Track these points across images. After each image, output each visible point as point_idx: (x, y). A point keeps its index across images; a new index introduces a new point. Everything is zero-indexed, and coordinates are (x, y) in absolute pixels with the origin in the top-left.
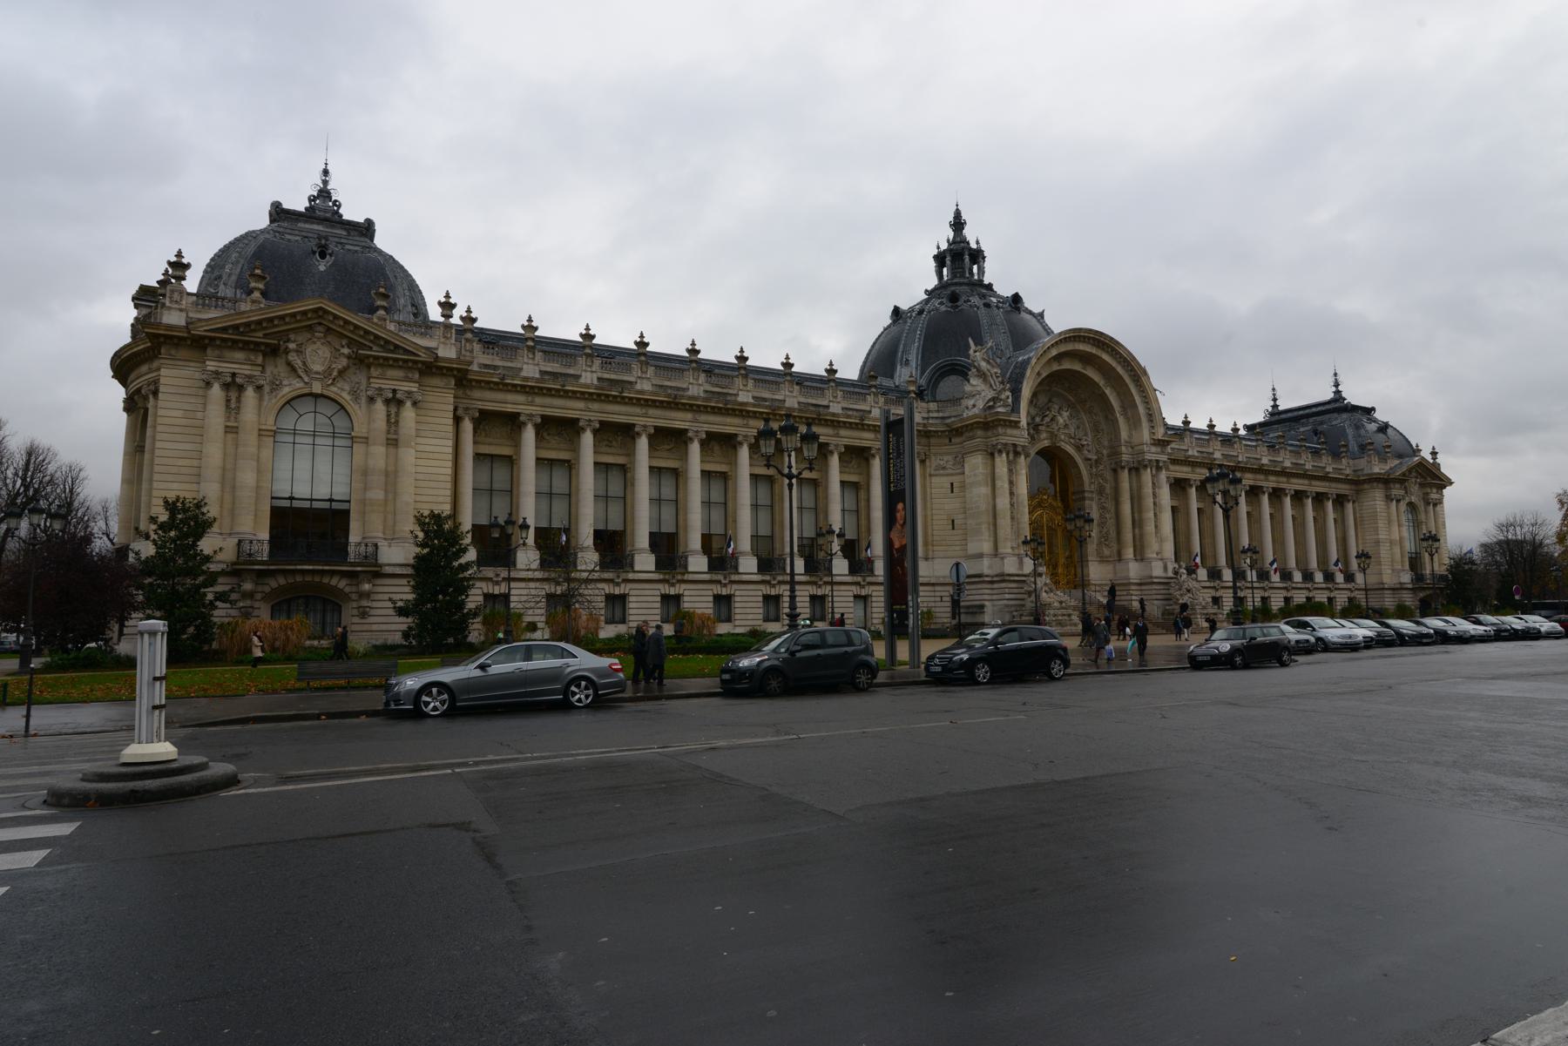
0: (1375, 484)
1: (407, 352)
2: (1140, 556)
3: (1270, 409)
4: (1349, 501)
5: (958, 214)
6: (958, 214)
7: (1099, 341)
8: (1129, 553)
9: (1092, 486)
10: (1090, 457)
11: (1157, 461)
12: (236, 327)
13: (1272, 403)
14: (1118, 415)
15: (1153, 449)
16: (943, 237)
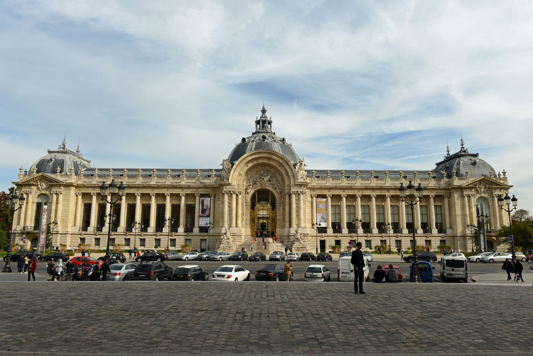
0: (455, 190)
1: (57, 182)
2: (290, 226)
3: (446, 156)
4: (445, 198)
5: (264, 109)
6: (264, 109)
7: (269, 152)
8: (287, 224)
9: (281, 201)
10: (278, 191)
11: (298, 192)
12: (27, 181)
13: (447, 153)
14: (285, 176)
15: (296, 187)
16: (259, 115)
